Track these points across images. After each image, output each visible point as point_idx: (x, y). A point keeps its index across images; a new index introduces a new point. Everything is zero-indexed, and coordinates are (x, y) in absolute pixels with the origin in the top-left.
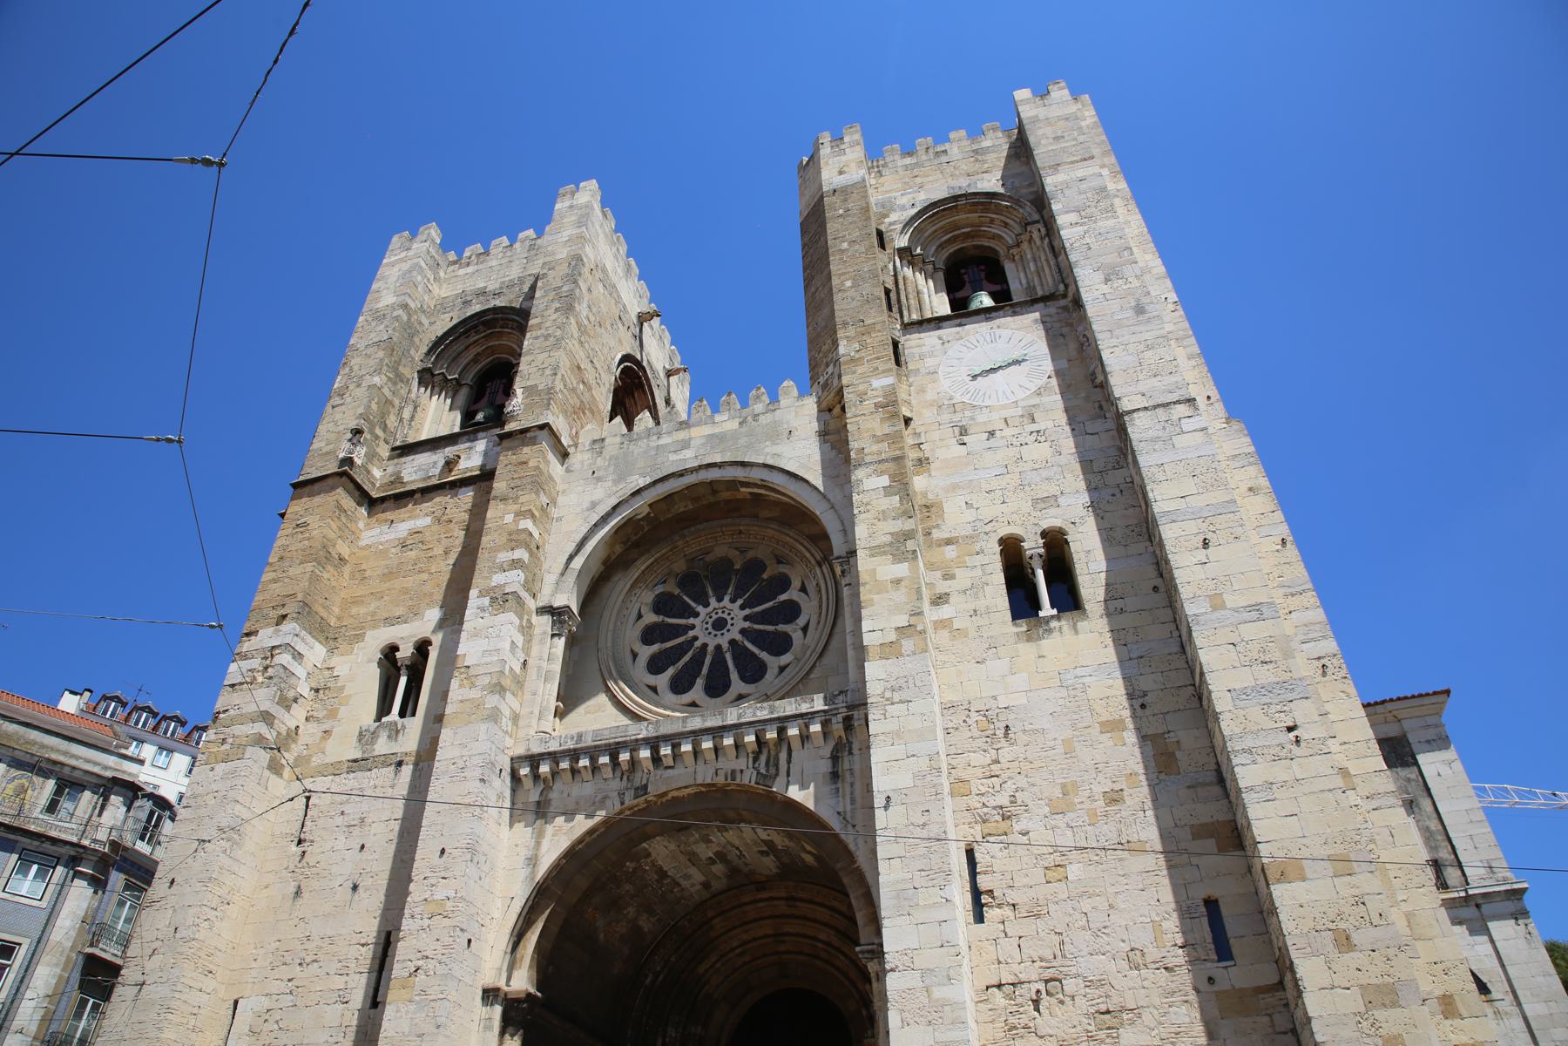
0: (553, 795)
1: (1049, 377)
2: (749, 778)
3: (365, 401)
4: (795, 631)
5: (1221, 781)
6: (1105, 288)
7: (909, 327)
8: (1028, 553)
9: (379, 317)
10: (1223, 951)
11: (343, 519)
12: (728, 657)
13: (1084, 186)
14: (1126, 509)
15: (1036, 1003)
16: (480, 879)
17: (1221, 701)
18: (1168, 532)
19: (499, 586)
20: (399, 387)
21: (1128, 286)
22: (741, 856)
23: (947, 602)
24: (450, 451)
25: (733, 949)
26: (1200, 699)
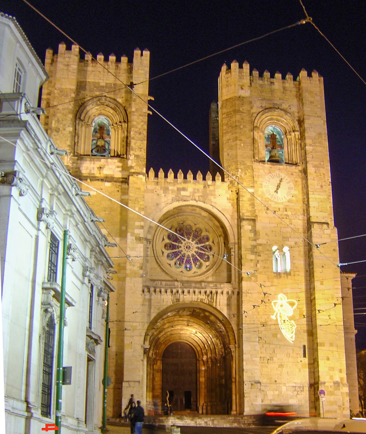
0: (153, 297)
1: (293, 196)
2: (206, 301)
4: (210, 255)
6: (314, 175)
10: (305, 356)
26: (311, 302)
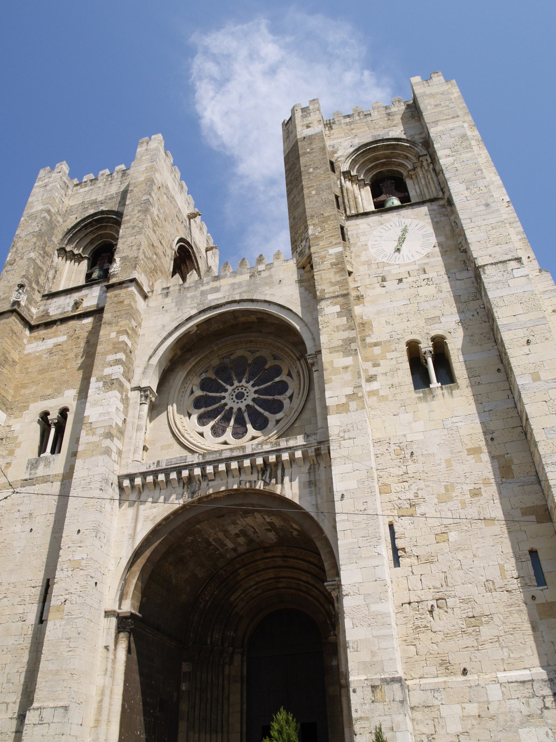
1: (434, 247)
3: (26, 267)
4: (285, 399)
5: (539, 482)
6: (467, 193)
7: (349, 218)
8: (423, 350)
9: (32, 217)
10: (541, 580)
11: (15, 338)
12: (246, 415)
13: (453, 133)
14: (481, 324)
15: (431, 612)
16: (101, 547)
17: (538, 435)
18: (506, 336)
19: (109, 375)
20: (46, 259)
21: (480, 192)
22: (255, 532)
23: (376, 380)
24: (76, 296)
25: (250, 587)
26: (526, 434)
